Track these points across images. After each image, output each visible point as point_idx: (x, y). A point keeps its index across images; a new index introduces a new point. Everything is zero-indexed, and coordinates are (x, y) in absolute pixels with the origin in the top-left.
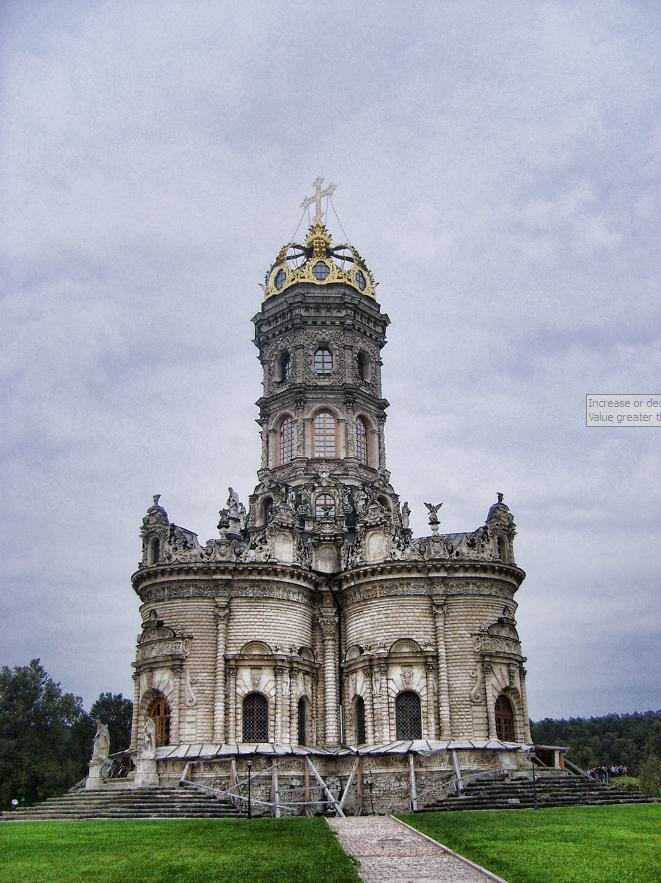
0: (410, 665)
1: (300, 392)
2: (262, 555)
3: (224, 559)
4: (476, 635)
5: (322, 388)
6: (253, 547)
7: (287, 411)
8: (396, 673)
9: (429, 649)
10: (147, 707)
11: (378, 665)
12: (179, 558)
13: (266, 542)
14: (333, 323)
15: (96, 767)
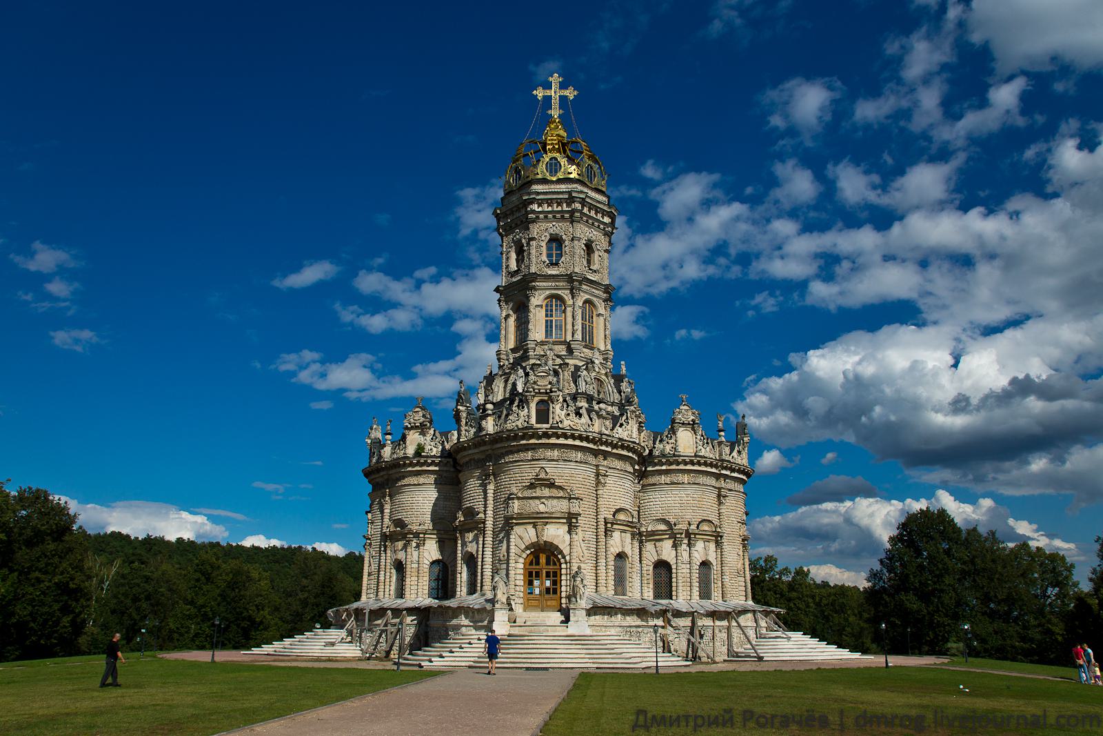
0: (708, 541)
1: (577, 280)
2: (626, 433)
3: (607, 432)
4: (740, 522)
5: (592, 282)
6: (621, 425)
7: (559, 292)
8: (700, 545)
9: (719, 530)
10: (524, 556)
11: (681, 536)
12: (571, 424)
13: (628, 423)
14: (599, 226)
15: (505, 612)
